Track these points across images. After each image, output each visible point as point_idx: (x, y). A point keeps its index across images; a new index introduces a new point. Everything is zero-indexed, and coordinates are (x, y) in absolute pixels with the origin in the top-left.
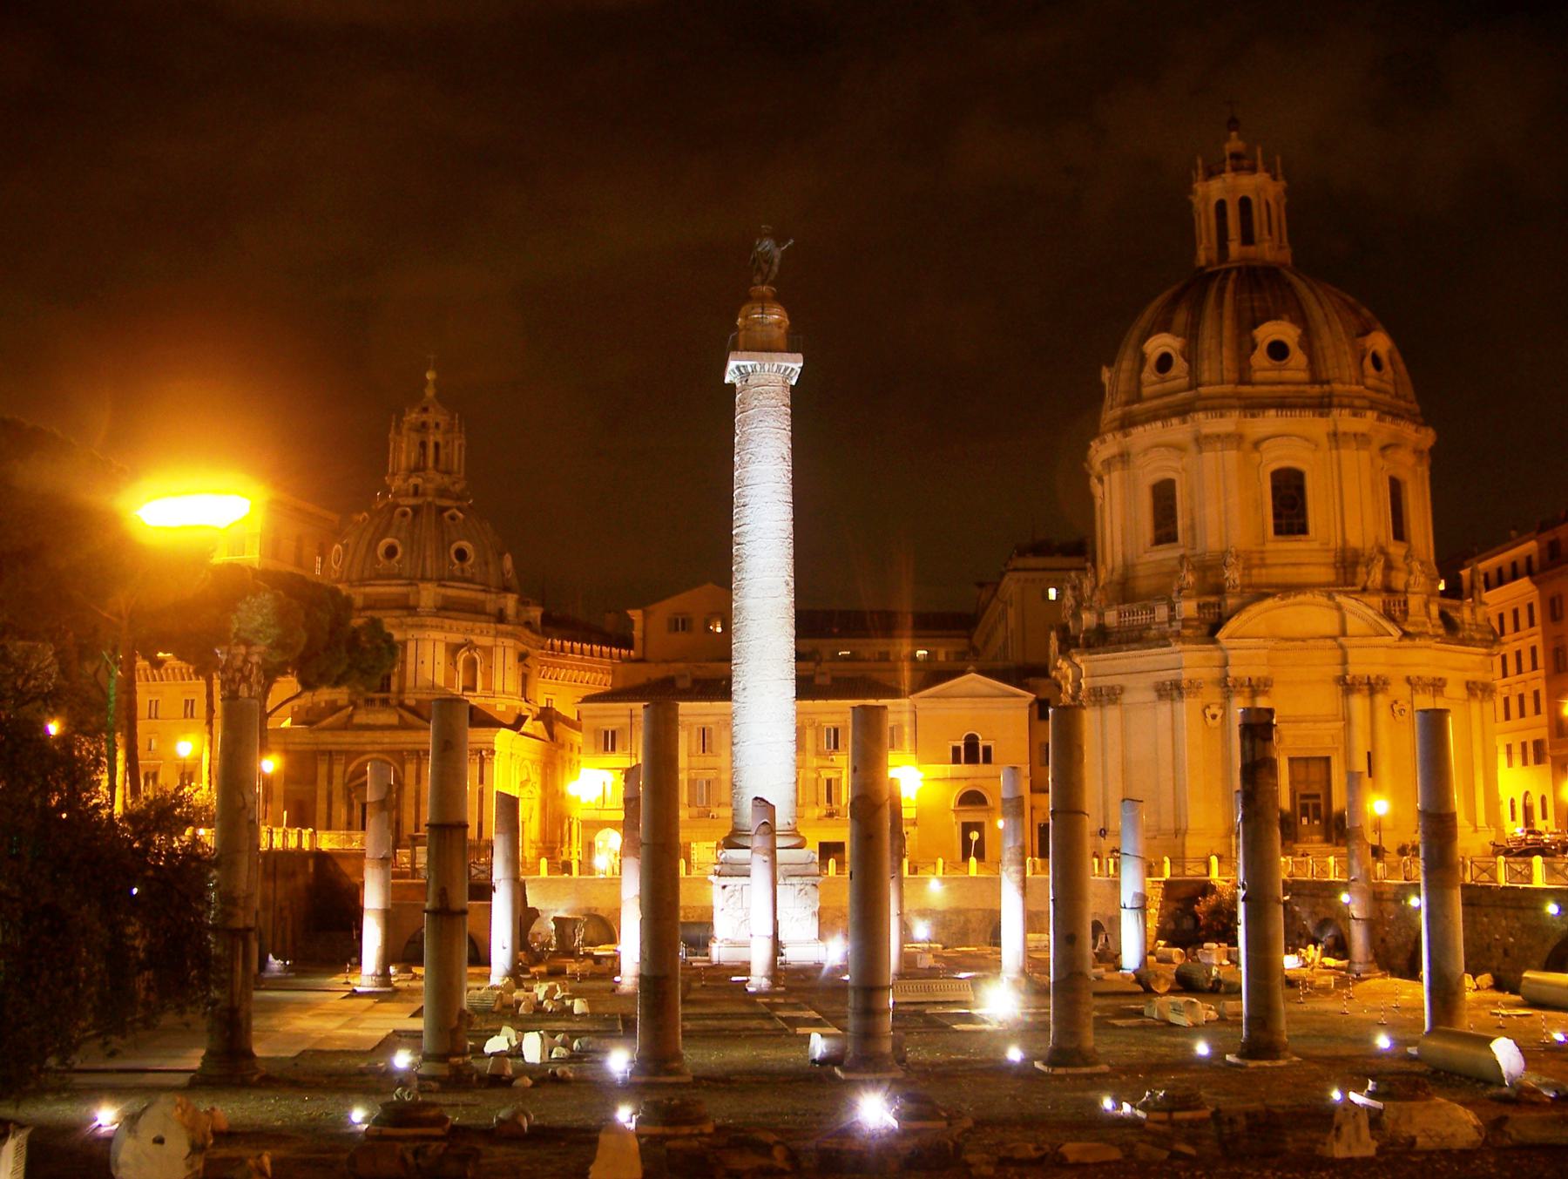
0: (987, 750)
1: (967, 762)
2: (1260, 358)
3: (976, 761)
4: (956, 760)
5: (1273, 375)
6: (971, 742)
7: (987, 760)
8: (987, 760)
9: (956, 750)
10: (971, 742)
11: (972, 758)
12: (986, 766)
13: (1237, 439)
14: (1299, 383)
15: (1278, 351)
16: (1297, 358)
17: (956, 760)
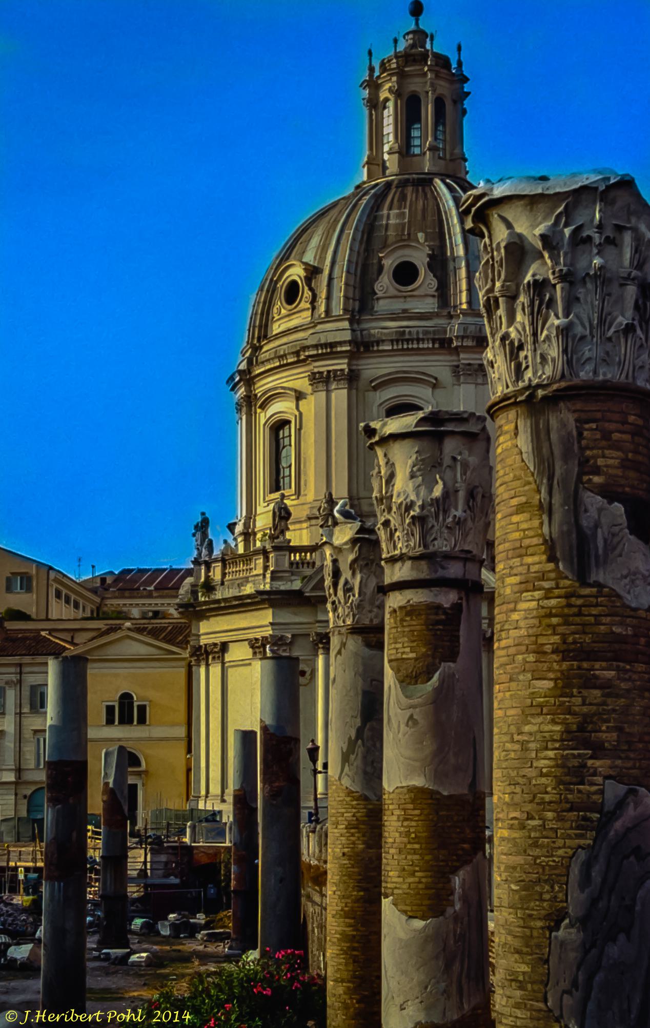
0: (142, 709)
1: (122, 722)
2: (385, 283)
3: (130, 722)
4: (110, 721)
5: (398, 306)
6: (126, 699)
7: (142, 720)
8: (142, 720)
9: (110, 710)
10: (126, 699)
11: (126, 720)
12: (141, 728)
13: (352, 378)
14: (422, 317)
15: (405, 274)
16: (426, 281)
17: (110, 721)
